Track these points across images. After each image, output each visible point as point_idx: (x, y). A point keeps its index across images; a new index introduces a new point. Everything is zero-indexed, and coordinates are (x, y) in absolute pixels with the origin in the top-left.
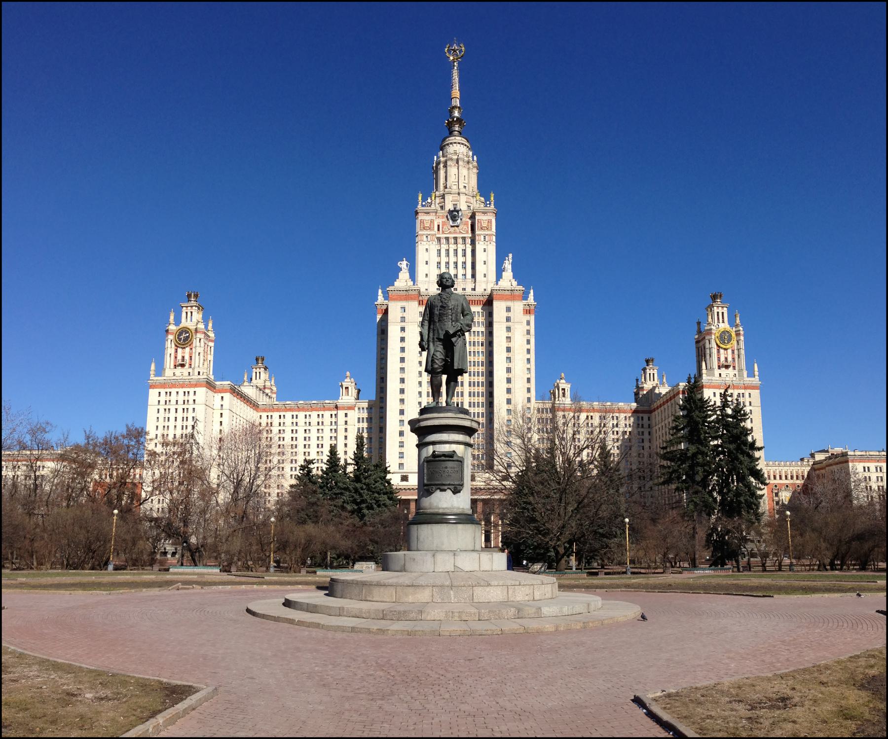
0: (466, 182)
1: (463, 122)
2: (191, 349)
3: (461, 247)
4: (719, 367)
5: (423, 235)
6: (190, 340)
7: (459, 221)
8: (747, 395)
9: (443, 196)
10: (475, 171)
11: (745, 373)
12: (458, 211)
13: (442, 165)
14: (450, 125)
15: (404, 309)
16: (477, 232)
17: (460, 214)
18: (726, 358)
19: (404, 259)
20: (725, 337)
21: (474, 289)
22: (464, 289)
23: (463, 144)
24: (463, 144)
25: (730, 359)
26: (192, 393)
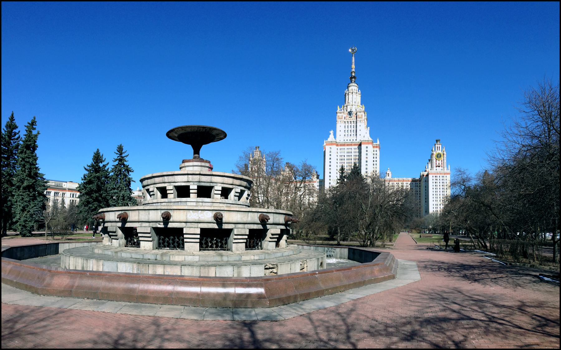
3: (352, 124)
4: (436, 167)
8: (445, 177)
9: (347, 106)
10: (360, 95)
11: (445, 168)
13: (347, 94)
14: (351, 78)
15: (331, 148)
16: (358, 119)
18: (439, 163)
20: (439, 156)
21: (356, 140)
22: (353, 140)
25: (440, 164)
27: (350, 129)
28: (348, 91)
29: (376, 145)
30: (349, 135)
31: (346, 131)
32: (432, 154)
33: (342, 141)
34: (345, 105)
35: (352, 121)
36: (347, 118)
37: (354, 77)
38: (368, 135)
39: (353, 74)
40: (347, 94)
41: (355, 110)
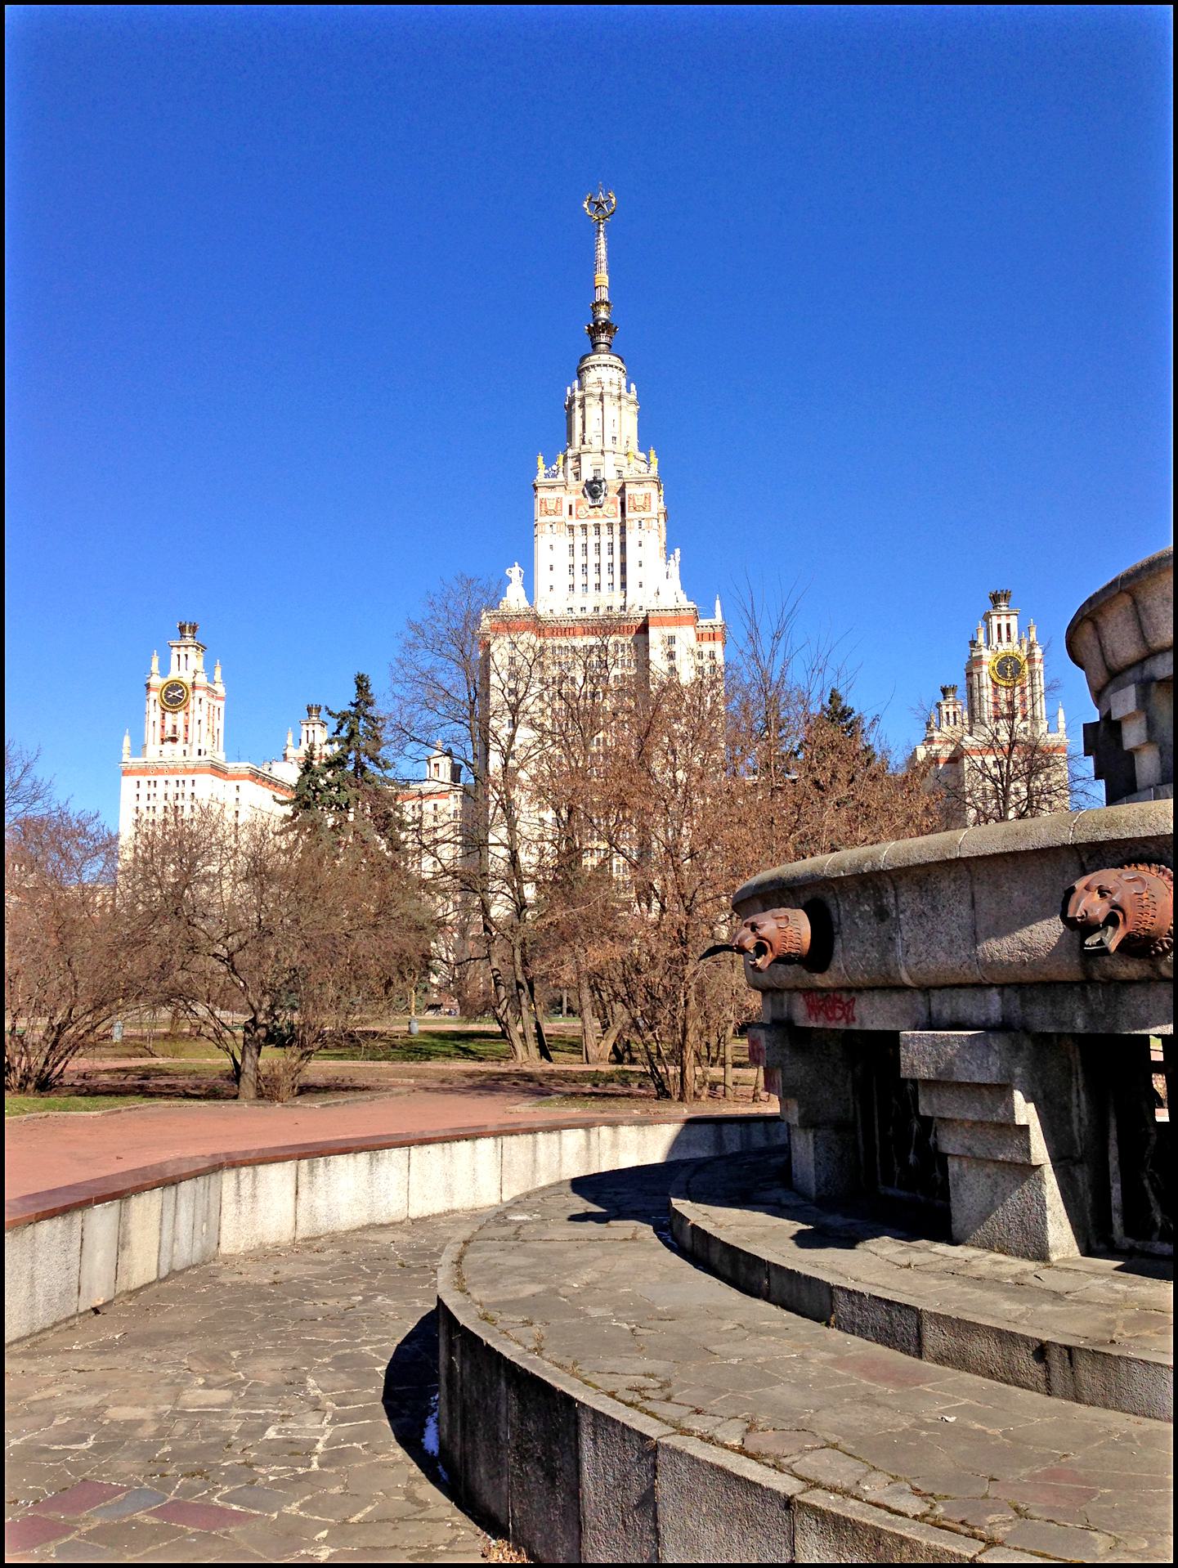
0: (617, 429)
1: (614, 326)
2: (187, 714)
3: (605, 539)
5: (544, 524)
6: (185, 701)
7: (602, 498)
9: (578, 458)
10: (634, 408)
12: (600, 483)
13: (577, 403)
14: (595, 331)
16: (628, 515)
17: (603, 487)
19: (516, 564)
20: (1009, 669)
23: (611, 366)
24: (611, 366)
26: (189, 783)
27: (593, 558)
28: (581, 388)
29: (711, 630)
30: (591, 587)
31: (578, 569)
32: (977, 661)
33: (560, 611)
34: (570, 452)
35: (603, 522)
36: (581, 508)
37: (607, 327)
38: (675, 582)
39: (603, 314)
40: (577, 403)
41: (615, 475)
